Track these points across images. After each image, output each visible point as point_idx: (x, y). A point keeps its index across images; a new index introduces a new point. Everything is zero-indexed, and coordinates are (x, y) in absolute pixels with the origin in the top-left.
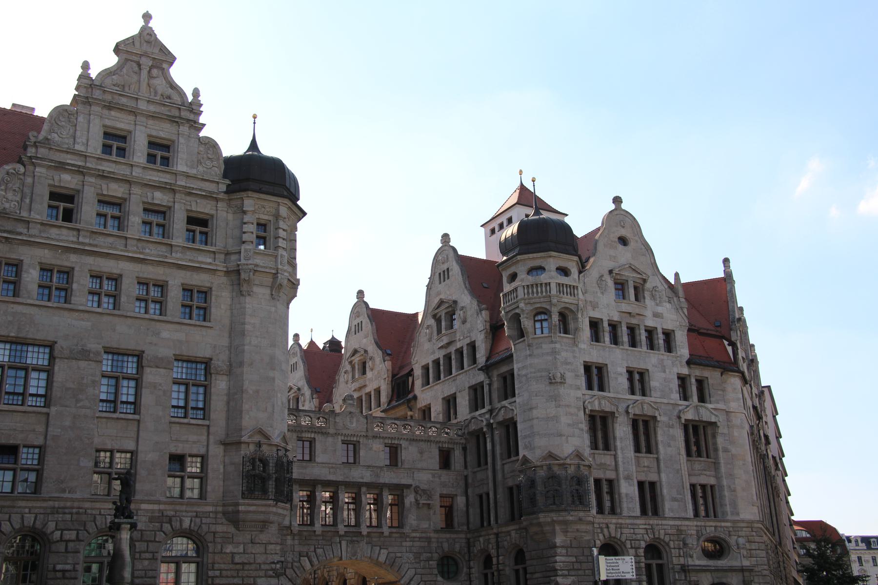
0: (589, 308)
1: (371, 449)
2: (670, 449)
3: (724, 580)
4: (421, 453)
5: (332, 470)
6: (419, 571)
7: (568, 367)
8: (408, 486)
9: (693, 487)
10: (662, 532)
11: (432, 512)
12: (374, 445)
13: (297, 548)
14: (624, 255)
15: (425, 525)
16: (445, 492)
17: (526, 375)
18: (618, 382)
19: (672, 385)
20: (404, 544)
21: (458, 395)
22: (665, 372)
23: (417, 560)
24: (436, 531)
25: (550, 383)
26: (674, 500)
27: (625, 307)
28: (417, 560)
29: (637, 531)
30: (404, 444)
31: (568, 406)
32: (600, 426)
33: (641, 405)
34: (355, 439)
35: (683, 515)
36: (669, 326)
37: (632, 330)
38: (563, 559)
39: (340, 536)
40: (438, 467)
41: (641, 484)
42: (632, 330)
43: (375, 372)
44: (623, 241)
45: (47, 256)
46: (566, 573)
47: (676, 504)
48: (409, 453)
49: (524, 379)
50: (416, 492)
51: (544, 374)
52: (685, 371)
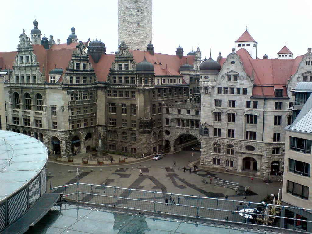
0: (218, 85)
3: (251, 157)
10: (232, 142)
13: (177, 131)
18: (225, 104)
22: (241, 101)
26: (239, 135)
27: (229, 83)
31: (205, 112)
32: (217, 116)
33: (232, 110)
37: (232, 89)
42: (232, 89)
45: (114, 90)
47: (240, 135)
52: (249, 100)
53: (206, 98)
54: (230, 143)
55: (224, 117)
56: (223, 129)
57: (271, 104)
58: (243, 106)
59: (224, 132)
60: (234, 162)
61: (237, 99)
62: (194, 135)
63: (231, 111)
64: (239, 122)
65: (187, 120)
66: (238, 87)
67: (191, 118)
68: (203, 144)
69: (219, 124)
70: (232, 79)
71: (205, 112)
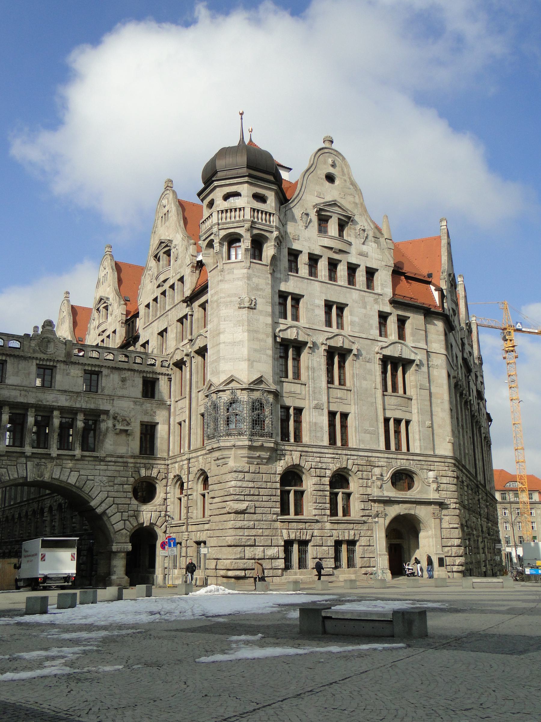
1: (68, 374)
2: (365, 382)
3: (412, 512)
4: (124, 380)
5: (23, 393)
6: (111, 494)
7: (259, 293)
8: (107, 412)
9: (387, 421)
10: (350, 462)
11: (130, 438)
12: (72, 371)
14: (331, 193)
15: (122, 450)
16: (146, 420)
17: (216, 301)
19: (371, 322)
20: (98, 467)
21: (169, 329)
22: (365, 308)
23: (111, 484)
24: (133, 457)
25: (240, 308)
28: (111, 484)
29: (323, 460)
30: (105, 372)
31: (256, 332)
34: (51, 364)
35: (374, 447)
36: (373, 265)
37: (333, 265)
38: (239, 484)
39: (27, 457)
40: (140, 395)
41: (332, 415)
42: (333, 265)
43: (113, 316)
44: (330, 178)
46: (242, 498)
48: (109, 382)
49: (215, 305)
50: (115, 418)
51: (233, 299)
52: (387, 308)
53: (259, 277)
54: (344, 466)
55: (313, 362)
56: (316, 408)
57: (438, 331)
58: (371, 328)
59: (314, 425)
60: (363, 541)
61: (353, 301)
62: (72, 480)
63: (340, 338)
64: (365, 384)
65: (45, 413)
66: (354, 260)
67: (63, 401)
68: (241, 476)
69: (296, 388)
70: (333, 227)
71: (256, 332)
